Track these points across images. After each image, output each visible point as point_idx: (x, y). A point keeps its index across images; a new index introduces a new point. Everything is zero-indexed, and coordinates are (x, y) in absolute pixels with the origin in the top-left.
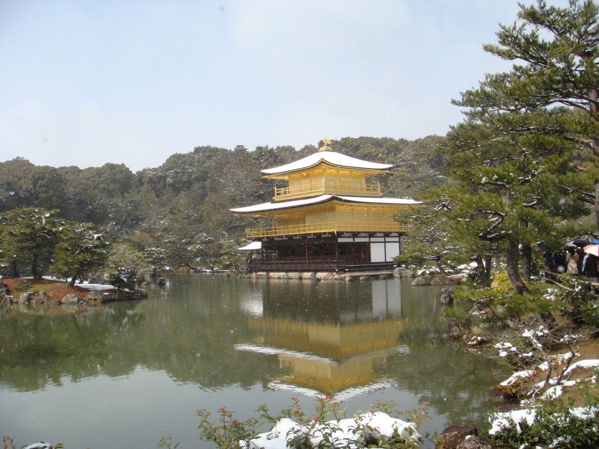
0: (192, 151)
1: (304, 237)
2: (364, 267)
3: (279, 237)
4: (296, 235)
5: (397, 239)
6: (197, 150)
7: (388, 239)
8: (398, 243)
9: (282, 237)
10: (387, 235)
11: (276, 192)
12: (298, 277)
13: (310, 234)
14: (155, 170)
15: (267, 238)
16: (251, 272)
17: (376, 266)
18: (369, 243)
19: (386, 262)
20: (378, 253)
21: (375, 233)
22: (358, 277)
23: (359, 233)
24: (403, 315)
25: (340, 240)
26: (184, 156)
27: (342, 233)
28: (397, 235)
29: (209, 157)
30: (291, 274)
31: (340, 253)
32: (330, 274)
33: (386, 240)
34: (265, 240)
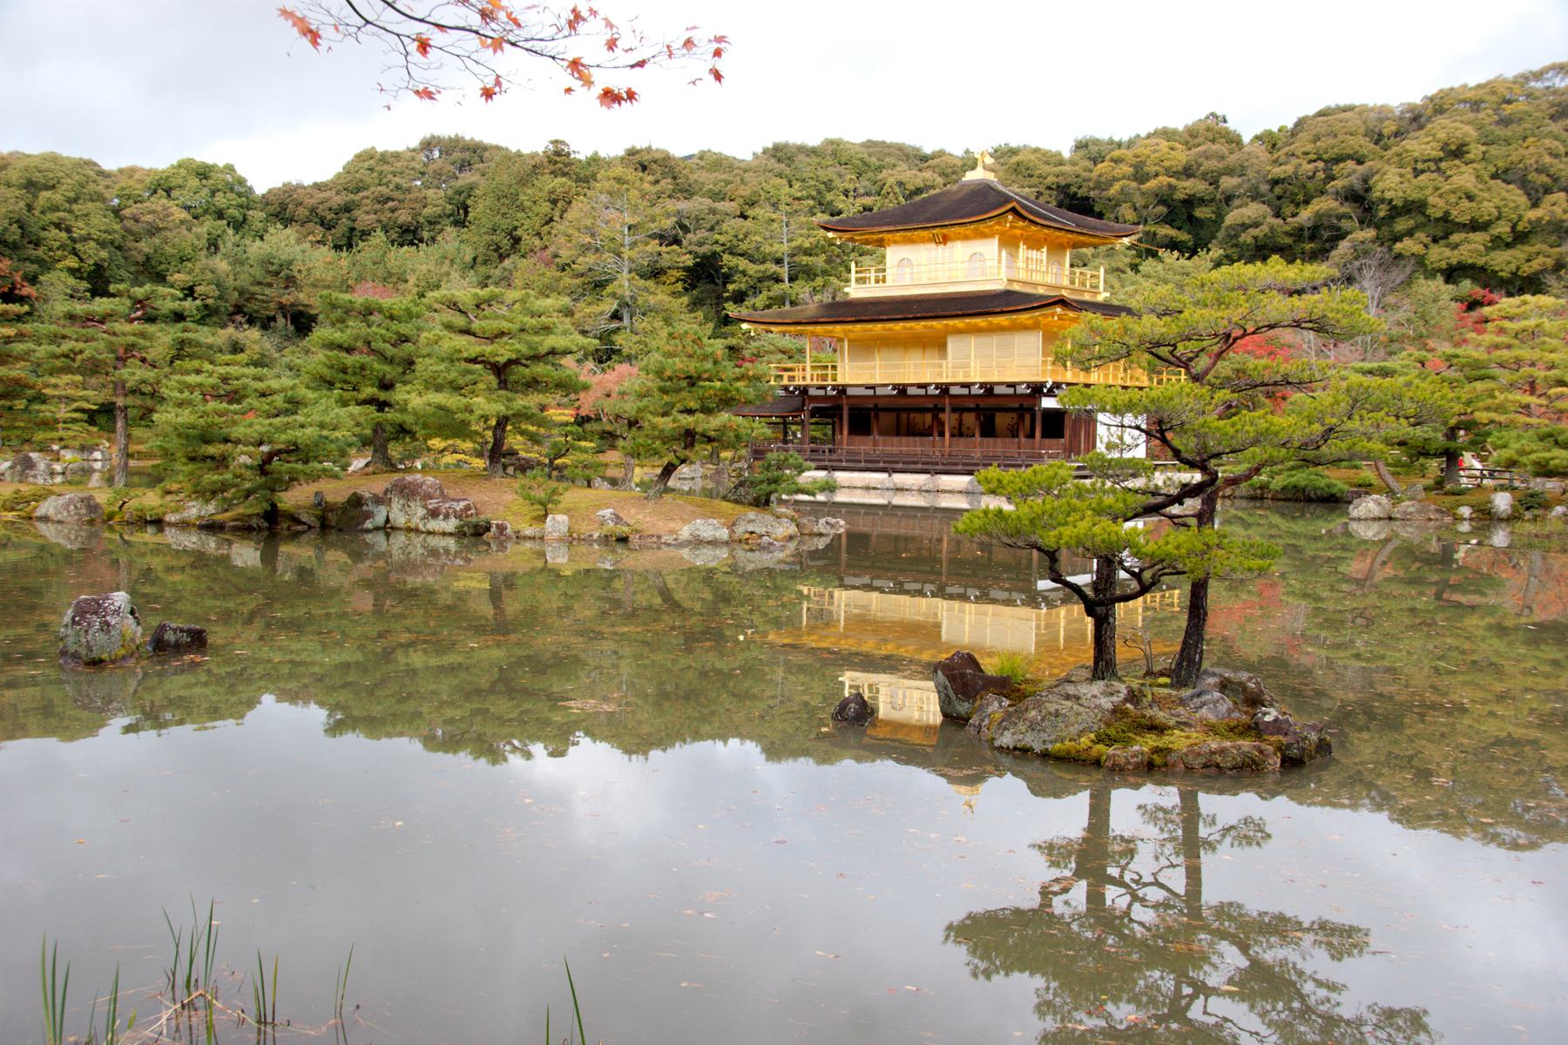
0: (415, 143)
1: (944, 389)
3: (868, 387)
4: (924, 386)
6: (428, 145)
9: (872, 387)
12: (930, 486)
14: (318, 187)
25: (1048, 403)
26: (397, 155)
29: (464, 165)
30: (899, 478)
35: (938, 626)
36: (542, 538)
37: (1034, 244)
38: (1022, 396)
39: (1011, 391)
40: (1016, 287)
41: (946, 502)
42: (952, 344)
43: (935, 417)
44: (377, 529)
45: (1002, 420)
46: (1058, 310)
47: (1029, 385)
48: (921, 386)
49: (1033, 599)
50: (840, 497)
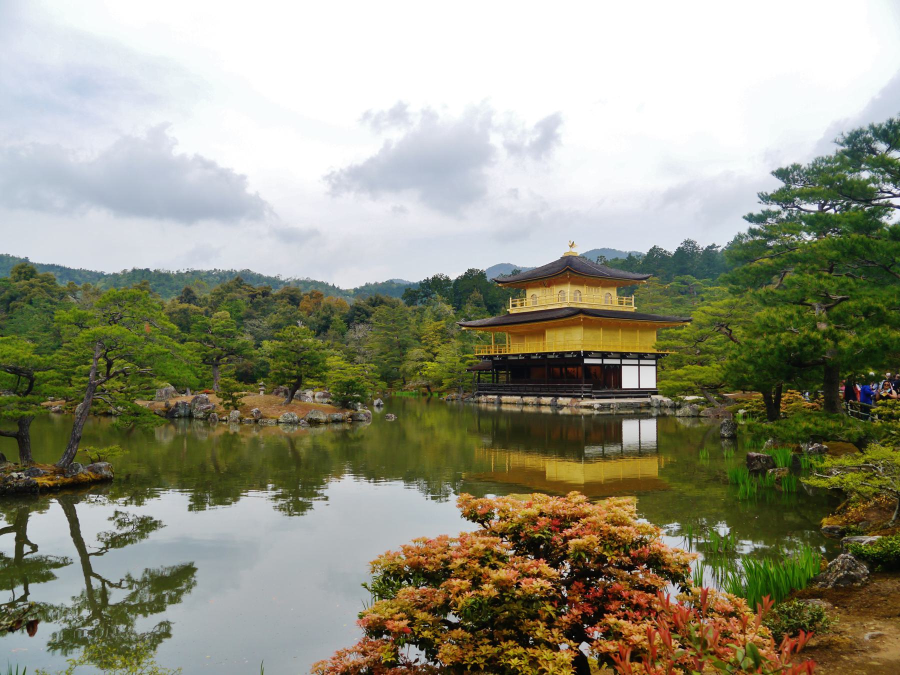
1: (544, 355)
2: (614, 393)
4: (534, 354)
5: (654, 362)
7: (642, 362)
9: (517, 355)
10: (641, 356)
13: (551, 353)
15: (500, 356)
16: (479, 395)
17: (629, 393)
18: (621, 365)
20: (630, 378)
21: (628, 354)
22: (610, 404)
23: (609, 353)
24: (658, 450)
25: (587, 361)
27: (590, 352)
28: (653, 356)
32: (574, 400)
34: (497, 359)
35: (545, 472)
42: (547, 333)
44: (185, 417)
46: (582, 316)
47: (575, 352)
49: (580, 456)
50: (504, 408)
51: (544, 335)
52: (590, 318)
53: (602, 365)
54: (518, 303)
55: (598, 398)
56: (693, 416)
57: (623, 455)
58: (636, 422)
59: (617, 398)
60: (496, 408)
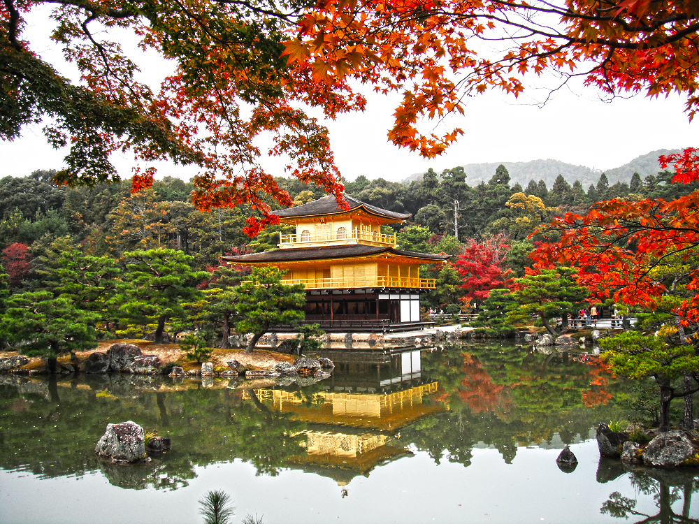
1: (330, 291)
5: (417, 297)
7: (413, 297)
8: (418, 301)
10: (412, 292)
11: (281, 238)
18: (400, 300)
19: (410, 322)
25: (381, 297)
31: (380, 313)
32: (373, 335)
33: (412, 298)
35: (330, 407)
36: (200, 374)
37: (366, 223)
38: (369, 294)
39: (363, 292)
40: (362, 243)
41: (334, 346)
43: (317, 305)
45: (351, 306)
47: (373, 289)
48: (318, 290)
49: (379, 391)
51: (329, 271)
52: (393, 255)
53: (389, 300)
54: (291, 238)
55: (394, 332)
56: (550, 345)
57: (405, 385)
58: (410, 353)
59: (406, 331)
60: (270, 346)
